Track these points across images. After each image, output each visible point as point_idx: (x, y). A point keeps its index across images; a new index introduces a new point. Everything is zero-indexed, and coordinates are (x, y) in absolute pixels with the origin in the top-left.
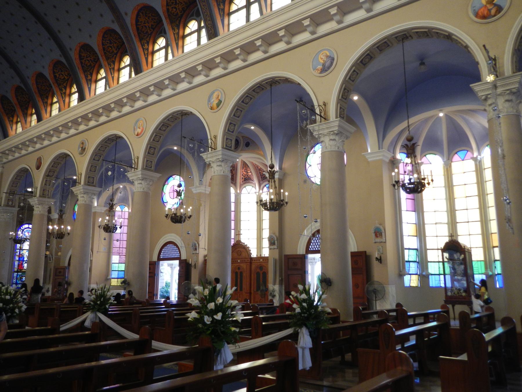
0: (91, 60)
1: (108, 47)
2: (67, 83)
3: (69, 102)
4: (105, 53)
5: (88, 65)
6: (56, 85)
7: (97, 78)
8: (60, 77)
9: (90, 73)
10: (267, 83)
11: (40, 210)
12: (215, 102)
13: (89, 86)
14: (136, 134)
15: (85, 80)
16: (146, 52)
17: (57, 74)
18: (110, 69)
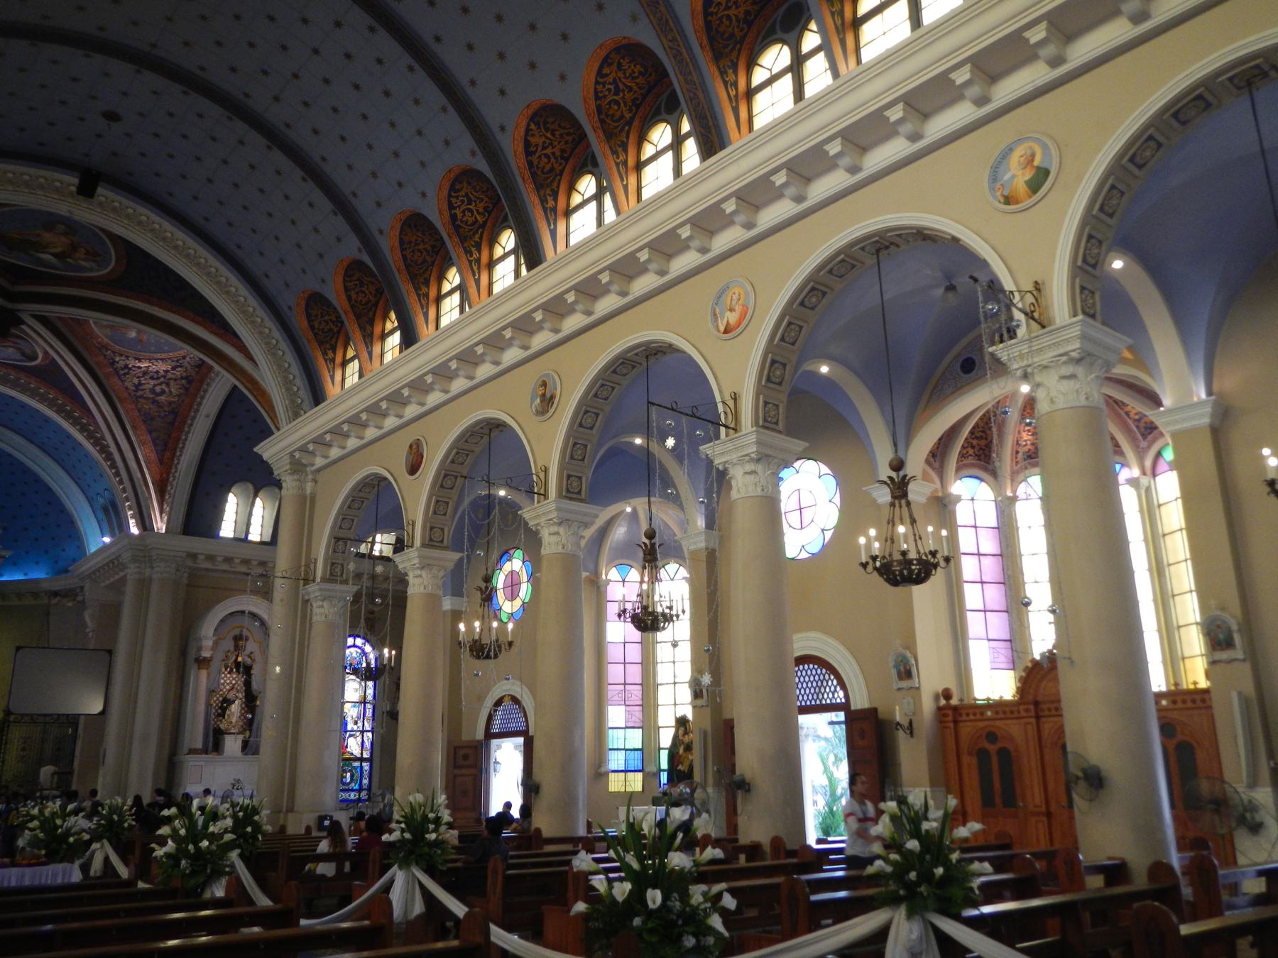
0: (553, 153)
1: (609, 103)
2: (482, 233)
3: (490, 284)
4: (602, 121)
5: (545, 170)
6: (457, 240)
7: (568, 204)
8: (464, 219)
9: (552, 190)
10: (1231, 79)
11: (426, 583)
12: (1017, 176)
13: (552, 227)
14: (722, 328)
15: (542, 212)
16: (733, 93)
17: (457, 211)
18: (617, 165)
